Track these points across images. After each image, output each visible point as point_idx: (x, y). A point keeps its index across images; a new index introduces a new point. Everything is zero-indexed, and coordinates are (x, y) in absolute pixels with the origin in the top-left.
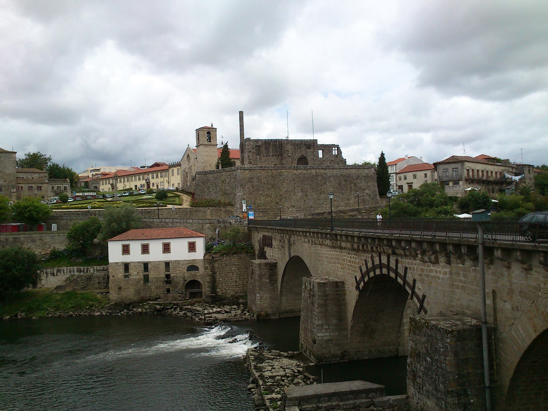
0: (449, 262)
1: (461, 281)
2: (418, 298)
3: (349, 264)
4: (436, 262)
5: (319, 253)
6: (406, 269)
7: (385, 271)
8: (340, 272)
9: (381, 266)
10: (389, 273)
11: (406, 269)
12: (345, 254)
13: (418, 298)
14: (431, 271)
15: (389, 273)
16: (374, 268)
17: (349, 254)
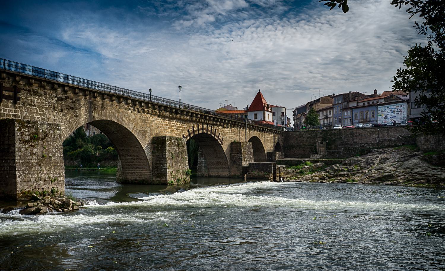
0: (231, 128)
1: (234, 133)
2: (220, 140)
3: (178, 128)
4: (227, 128)
5: (148, 120)
6: (216, 130)
7: (205, 131)
8: (169, 133)
9: (203, 129)
10: (207, 132)
11: (216, 130)
12: (175, 122)
13: (220, 140)
14: (225, 130)
15: (207, 132)
16: (198, 130)
17: (178, 122)
